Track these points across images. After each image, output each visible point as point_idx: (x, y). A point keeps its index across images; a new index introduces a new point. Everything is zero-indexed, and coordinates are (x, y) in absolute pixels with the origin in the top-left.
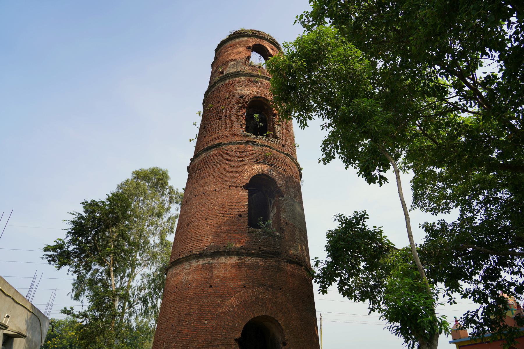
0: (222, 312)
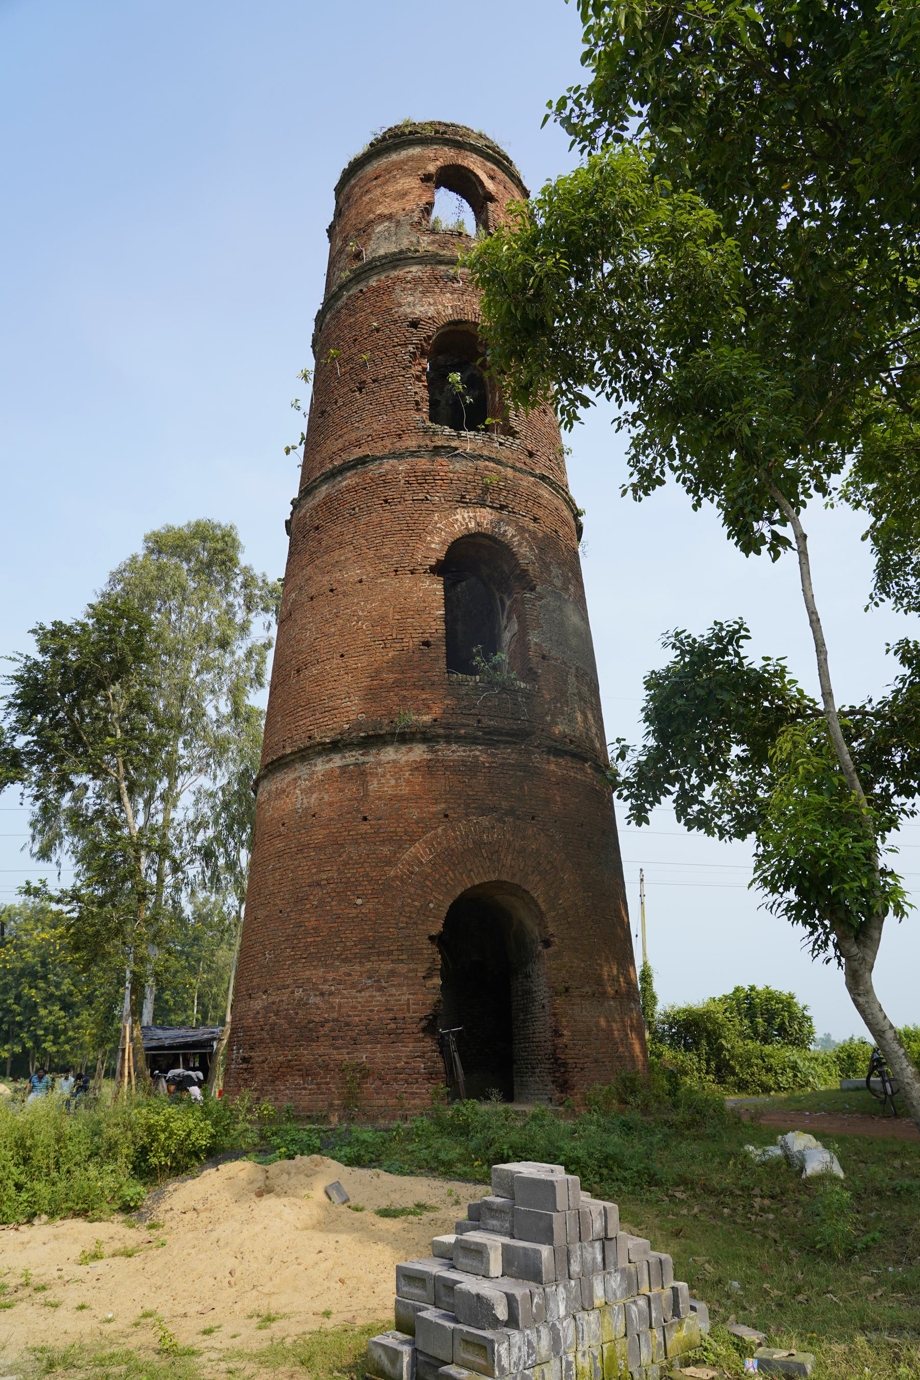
0: (396, 877)
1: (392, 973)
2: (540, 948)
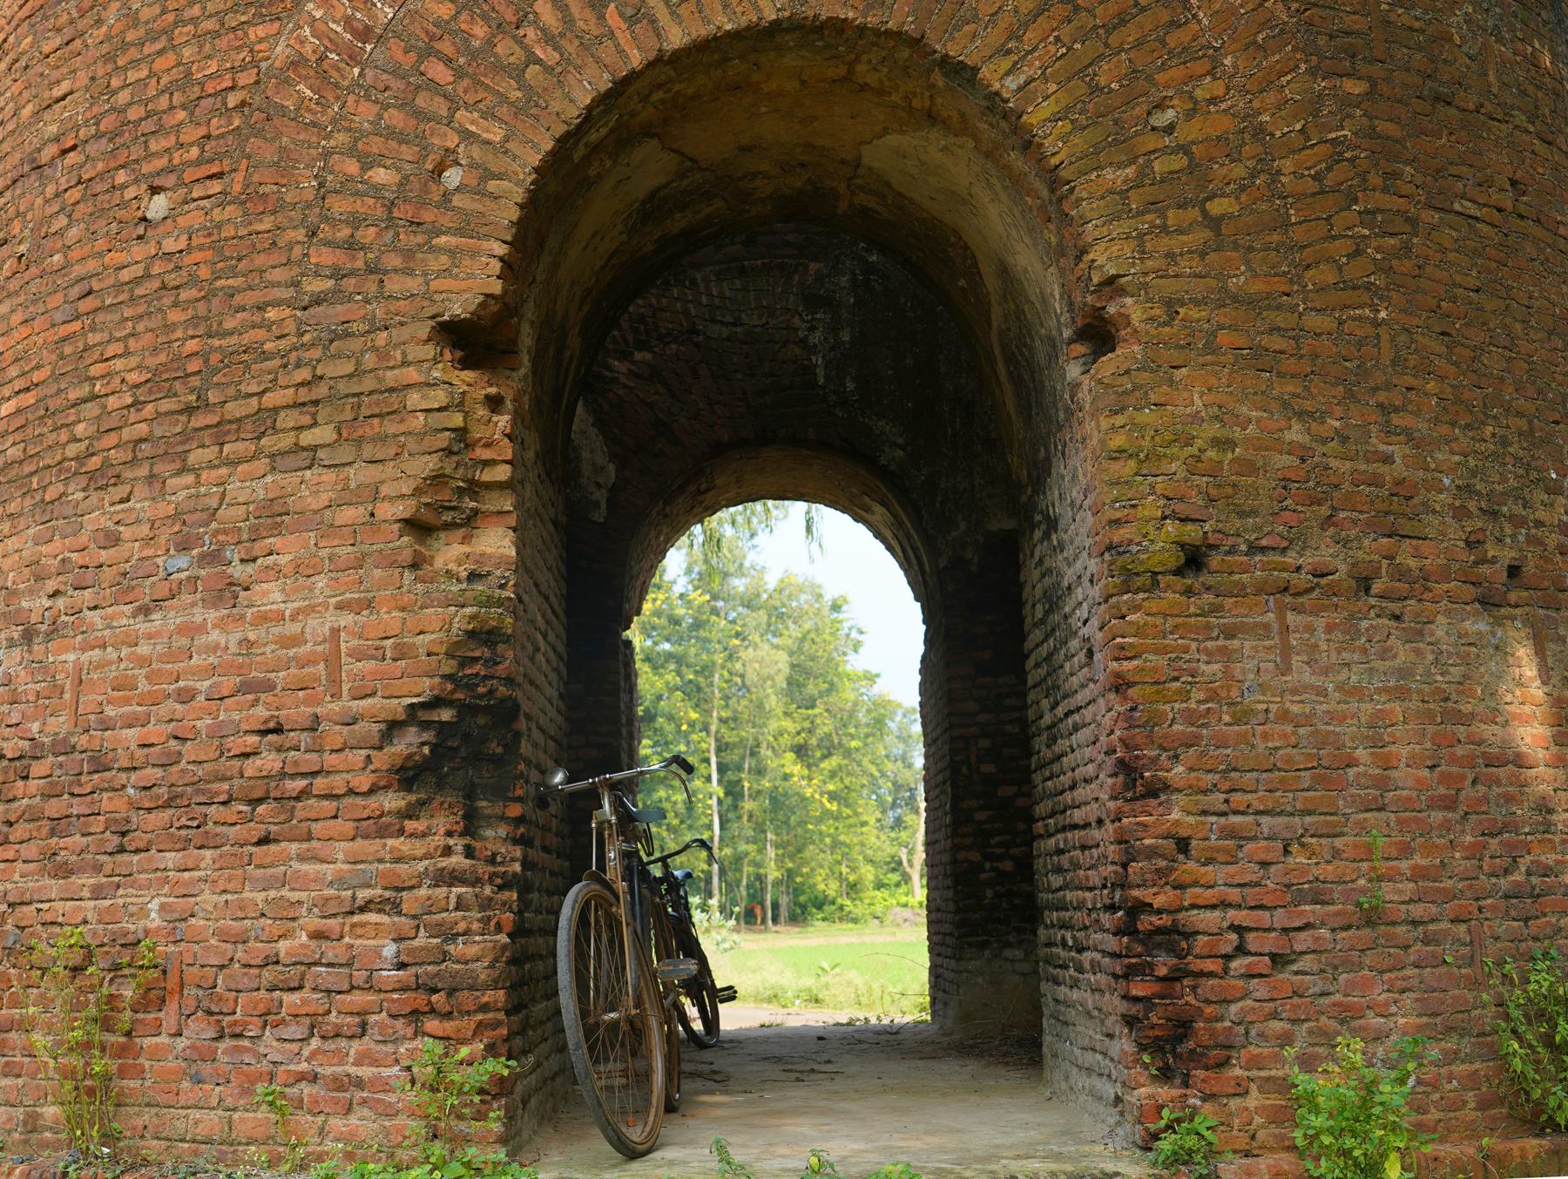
0: (297, 63)
1: (274, 516)
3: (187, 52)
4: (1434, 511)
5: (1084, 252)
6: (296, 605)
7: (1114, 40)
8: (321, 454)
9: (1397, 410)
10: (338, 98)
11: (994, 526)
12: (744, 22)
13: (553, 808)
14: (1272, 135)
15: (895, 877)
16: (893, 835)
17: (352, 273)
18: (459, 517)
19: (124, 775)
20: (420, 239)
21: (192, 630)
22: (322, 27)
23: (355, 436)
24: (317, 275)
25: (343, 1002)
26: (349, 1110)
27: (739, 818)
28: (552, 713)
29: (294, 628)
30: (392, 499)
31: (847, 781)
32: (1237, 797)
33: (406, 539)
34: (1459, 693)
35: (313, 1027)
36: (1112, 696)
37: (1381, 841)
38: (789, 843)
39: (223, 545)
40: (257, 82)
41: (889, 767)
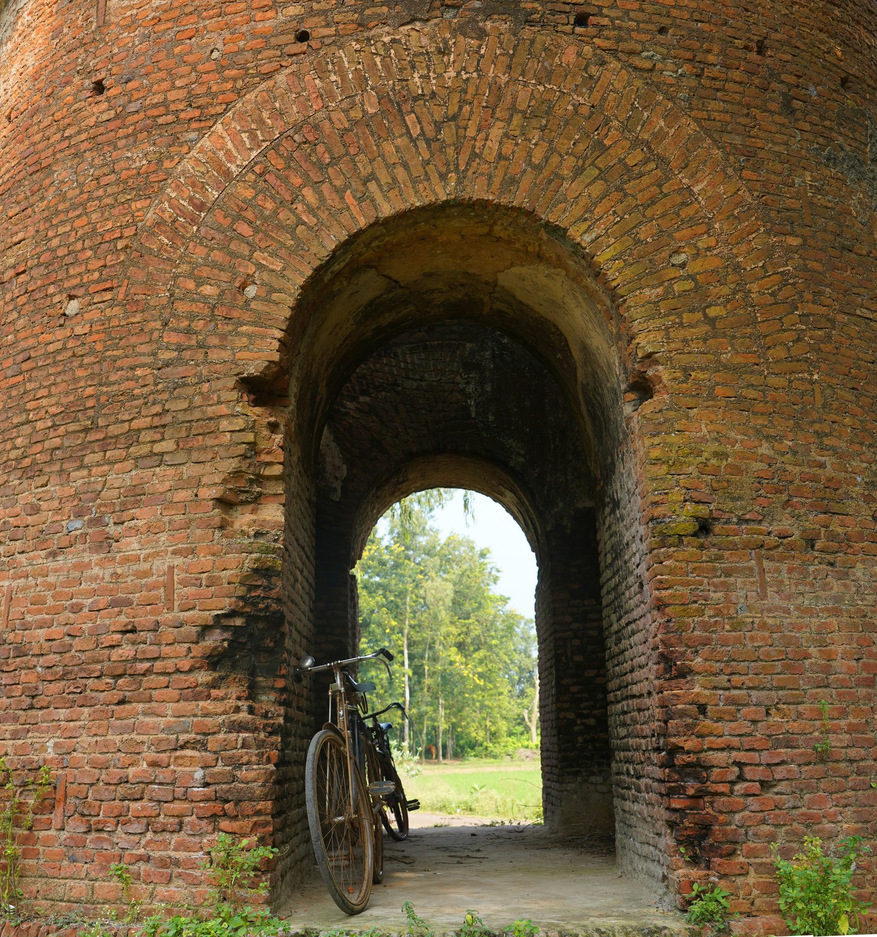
1: (136, 495)
2: (628, 409)
3: (94, 217)
4: (852, 498)
5: (632, 338)
6: (147, 551)
7: (648, 213)
8: (166, 458)
9: (826, 435)
10: (183, 244)
11: (580, 505)
12: (427, 201)
13: (304, 682)
14: (745, 269)
15: (520, 729)
16: (519, 701)
17: (188, 348)
18: (250, 497)
19: (35, 659)
20: (230, 328)
21: (81, 567)
22: (176, 202)
23: (187, 446)
24: (167, 348)
25: (168, 809)
26: (170, 881)
27: (422, 689)
28: (305, 621)
29: (145, 566)
30: (209, 486)
31: (490, 666)
32: (735, 678)
33: (217, 510)
34: (873, 612)
35: (148, 825)
36: (655, 612)
37: (828, 707)
38: (453, 706)
39: (103, 513)
40: (135, 234)
41: (516, 657)
